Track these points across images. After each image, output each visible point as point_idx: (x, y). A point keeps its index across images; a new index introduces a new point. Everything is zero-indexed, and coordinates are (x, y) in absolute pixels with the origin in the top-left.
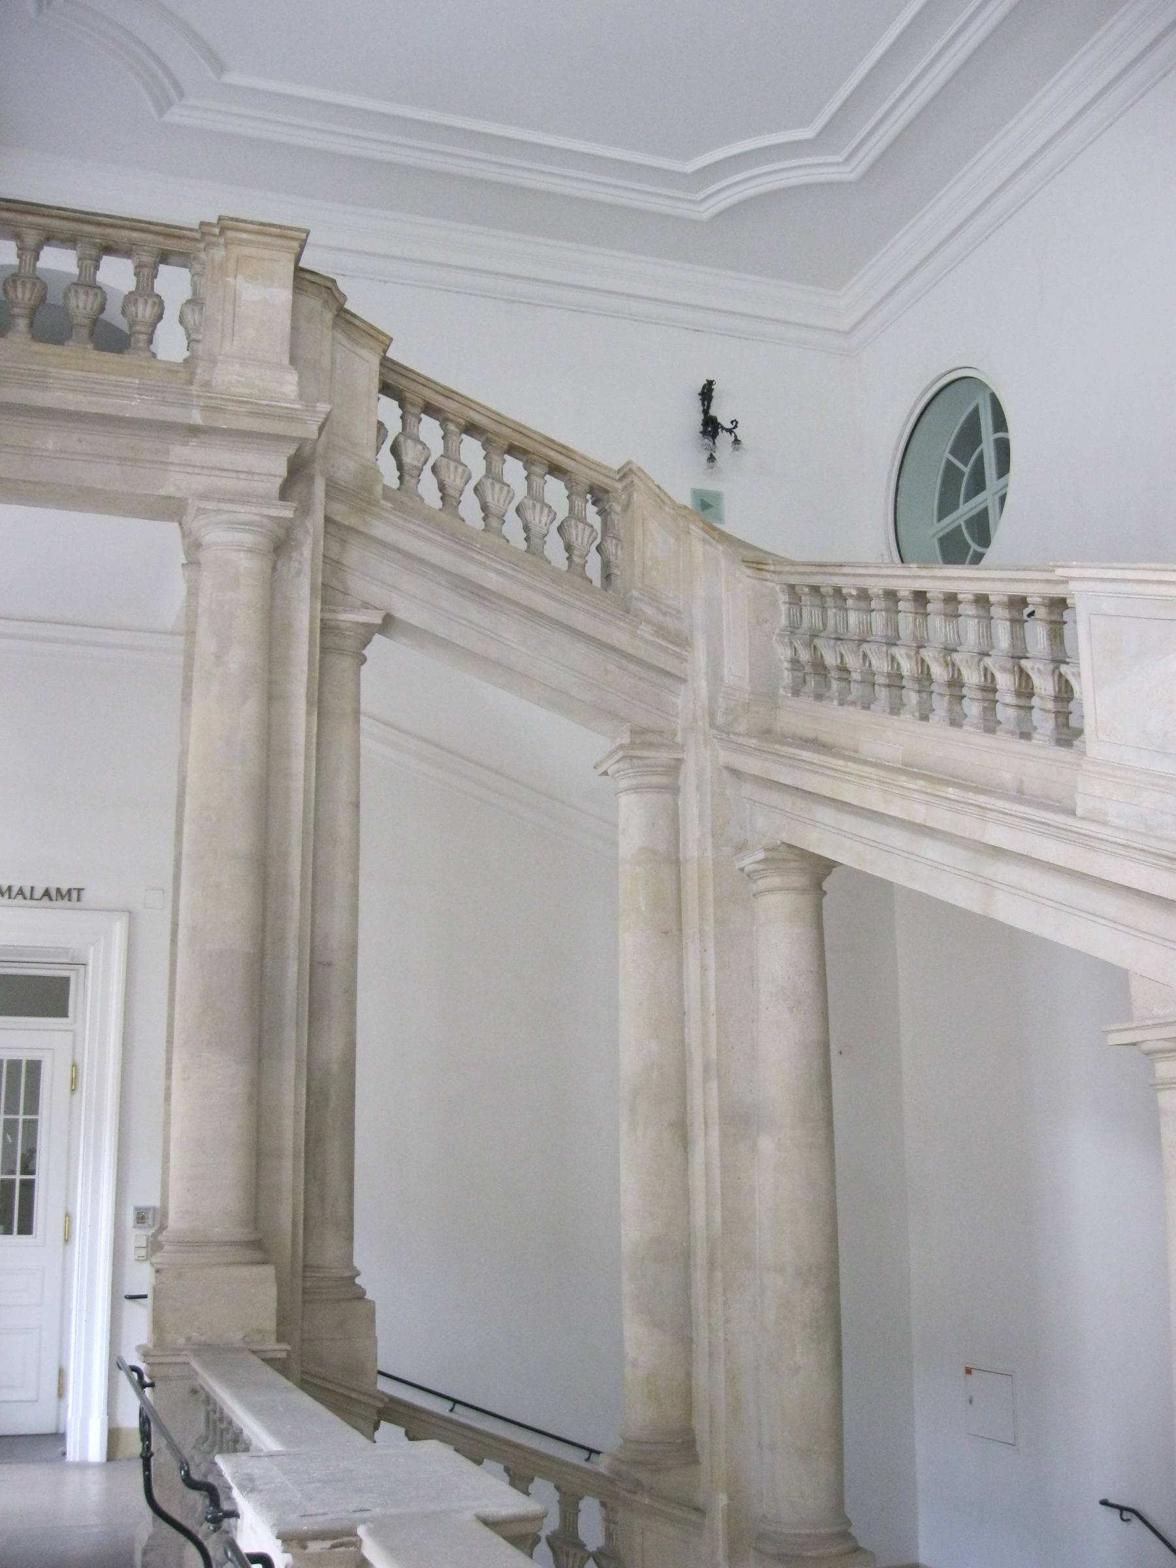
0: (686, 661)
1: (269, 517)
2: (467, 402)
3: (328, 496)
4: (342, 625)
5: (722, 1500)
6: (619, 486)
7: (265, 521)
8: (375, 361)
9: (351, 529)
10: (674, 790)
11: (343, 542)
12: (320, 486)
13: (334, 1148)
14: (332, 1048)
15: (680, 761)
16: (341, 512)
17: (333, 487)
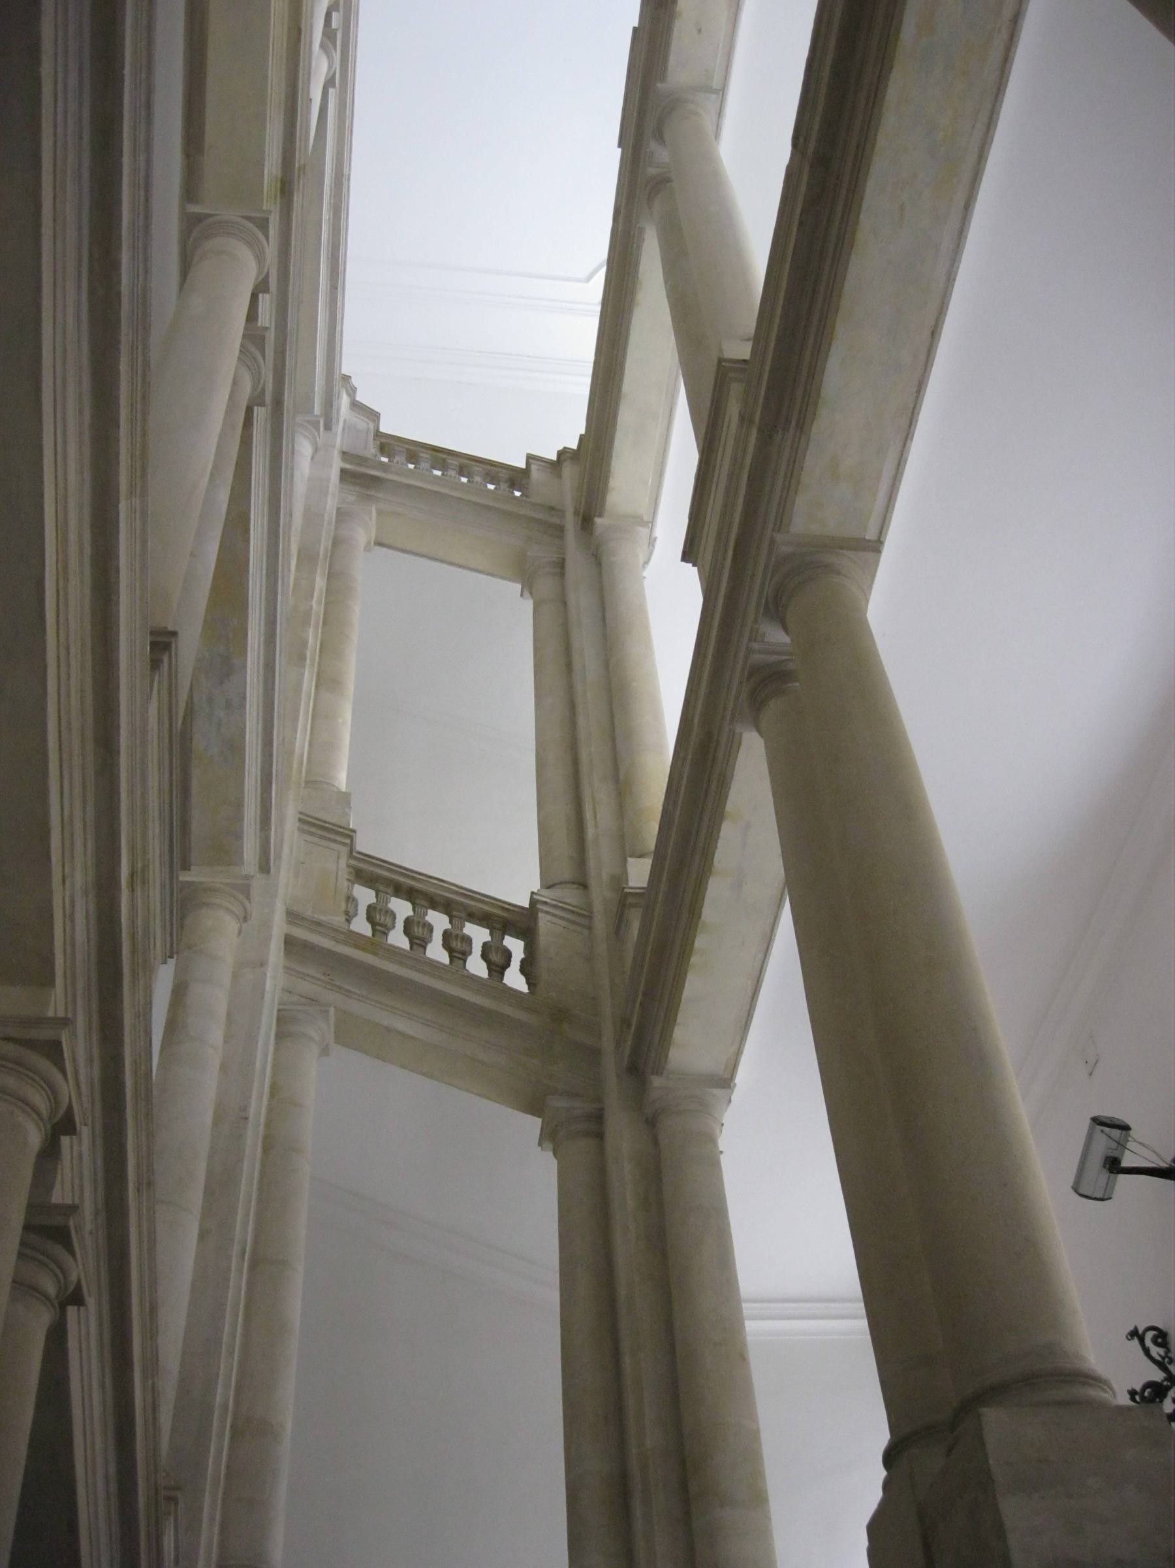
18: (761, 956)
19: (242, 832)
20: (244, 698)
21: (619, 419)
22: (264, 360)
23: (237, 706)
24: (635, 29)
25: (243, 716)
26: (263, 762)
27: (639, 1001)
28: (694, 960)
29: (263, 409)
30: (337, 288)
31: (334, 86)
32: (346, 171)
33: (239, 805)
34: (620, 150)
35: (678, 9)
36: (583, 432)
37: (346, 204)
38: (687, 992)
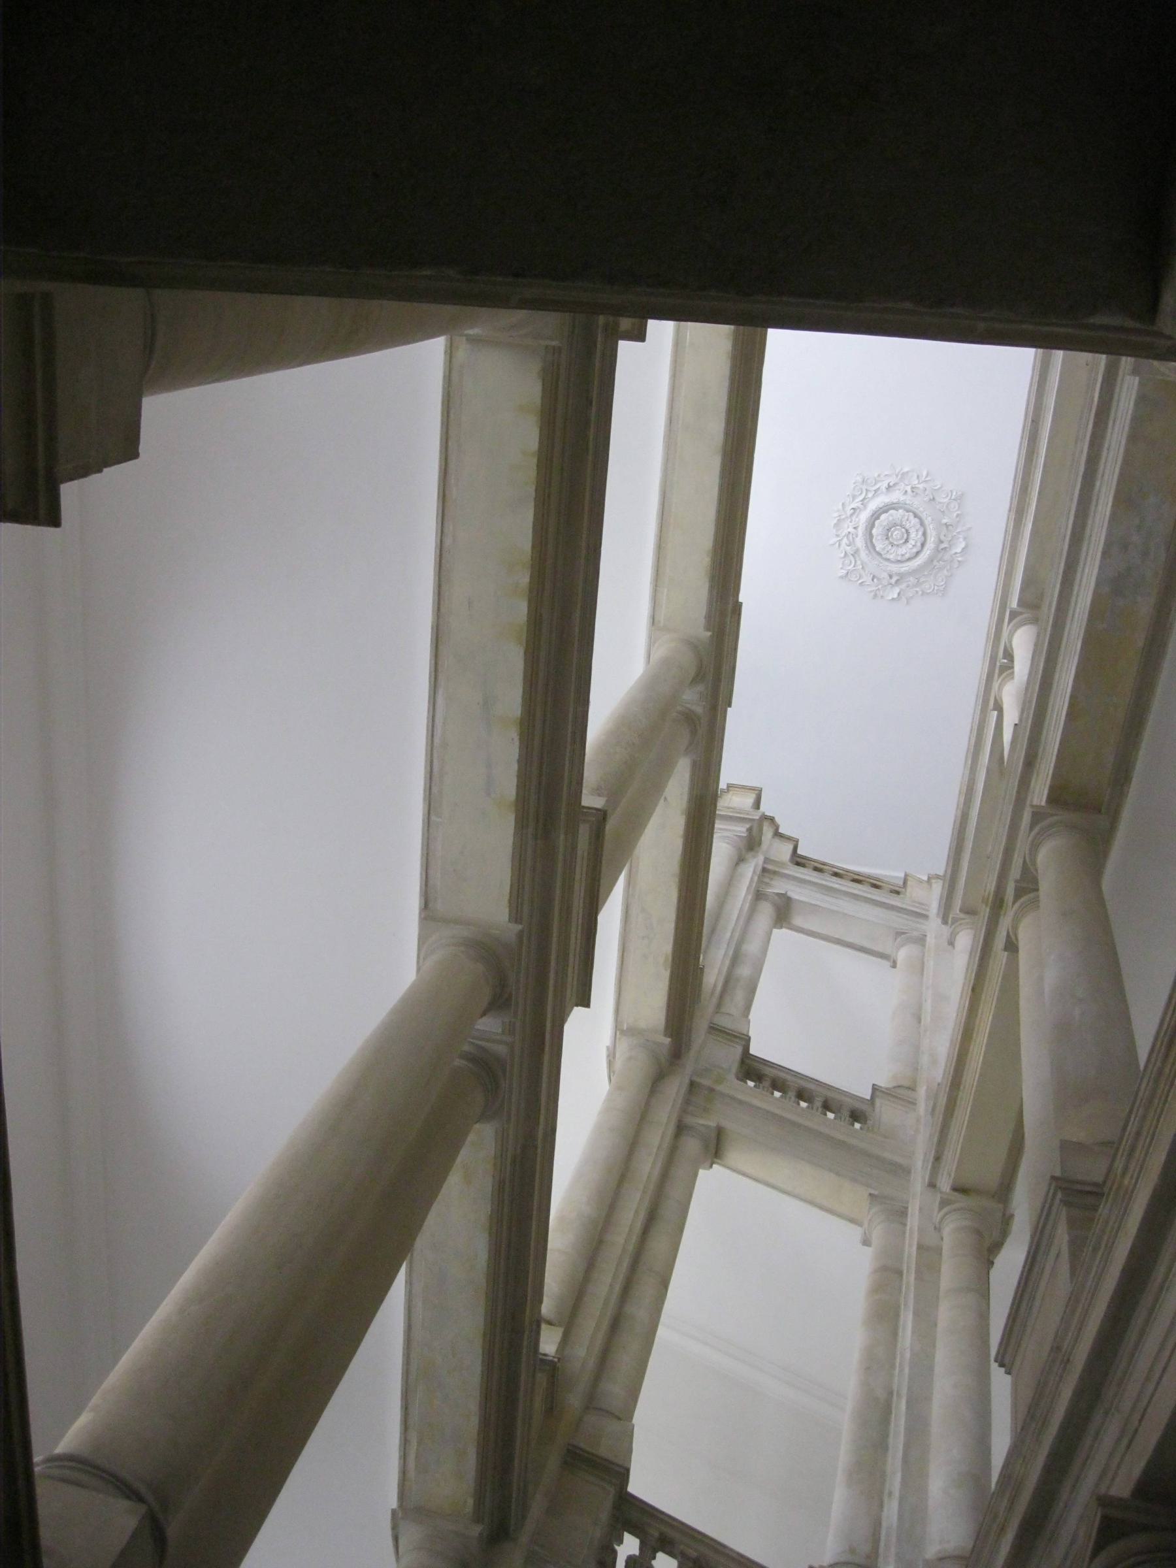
0: (928, 911)
1: (736, 835)
2: (833, 866)
3: (765, 862)
4: (768, 893)
5: (925, 1088)
6: (903, 890)
7: (735, 837)
8: (791, 847)
9: (775, 873)
10: (924, 946)
11: (772, 879)
12: (760, 859)
13: (739, 996)
14: (744, 971)
15: (926, 936)
16: (770, 867)
17: (767, 860)
18: (448, 542)
19: (1137, 404)
20: (1106, 553)
21: (723, 425)
22: (1025, 858)
23: (1115, 545)
24: (730, 705)
25: (1109, 534)
26: (1103, 437)
27: (594, 409)
28: (524, 579)
29: (1035, 802)
30: (1033, 421)
31: (1010, 612)
32: (1012, 524)
33: (1134, 437)
34: (740, 600)
35: (684, 816)
36: (729, 709)
37: (1015, 490)
38: (528, 516)
